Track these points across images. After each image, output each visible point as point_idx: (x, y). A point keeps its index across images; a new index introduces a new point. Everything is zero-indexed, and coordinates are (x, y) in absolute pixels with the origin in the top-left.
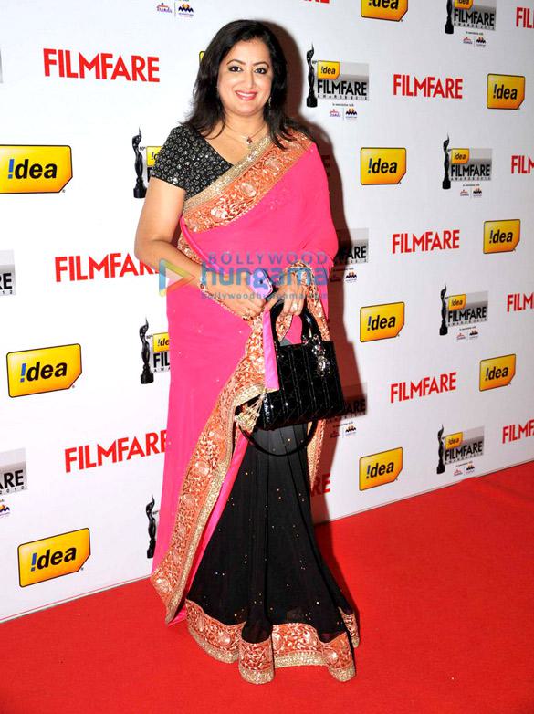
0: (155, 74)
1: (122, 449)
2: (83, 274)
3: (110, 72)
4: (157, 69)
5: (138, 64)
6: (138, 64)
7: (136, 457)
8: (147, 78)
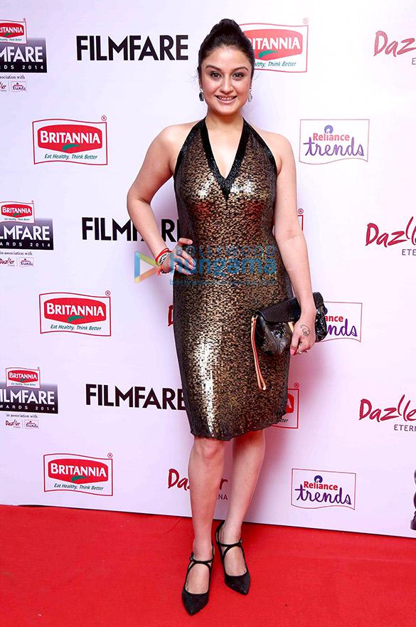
0: (183, 53)
1: (138, 397)
2: (107, 235)
3: (137, 53)
4: (186, 47)
5: (167, 43)
6: (167, 43)
7: (152, 407)
8: (174, 55)
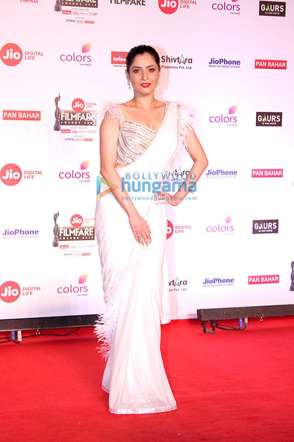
0: (144, 3)
8: (141, 4)
